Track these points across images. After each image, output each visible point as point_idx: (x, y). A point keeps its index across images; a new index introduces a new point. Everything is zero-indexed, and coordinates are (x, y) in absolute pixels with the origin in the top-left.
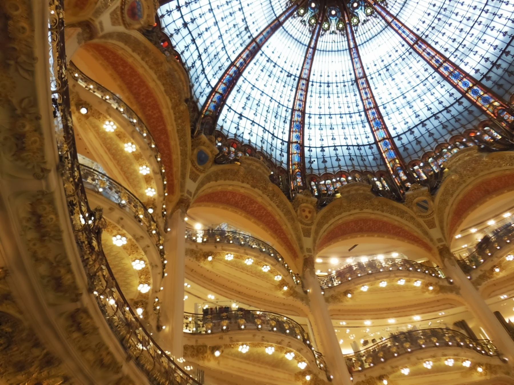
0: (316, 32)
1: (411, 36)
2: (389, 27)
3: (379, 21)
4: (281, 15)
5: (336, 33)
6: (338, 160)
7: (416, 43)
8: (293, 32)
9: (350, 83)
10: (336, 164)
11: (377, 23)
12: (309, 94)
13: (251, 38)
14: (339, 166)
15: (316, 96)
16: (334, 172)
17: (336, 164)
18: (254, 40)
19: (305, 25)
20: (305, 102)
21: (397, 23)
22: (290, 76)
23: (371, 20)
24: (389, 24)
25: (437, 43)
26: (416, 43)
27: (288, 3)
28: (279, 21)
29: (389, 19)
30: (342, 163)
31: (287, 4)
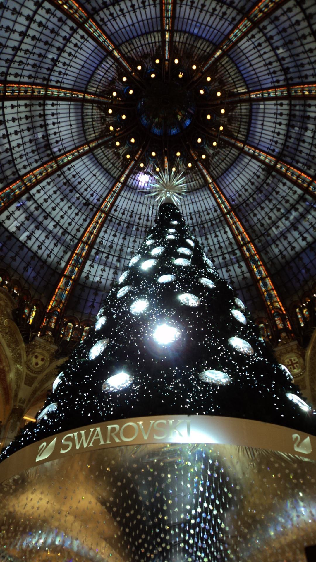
3: (198, 178)
8: (104, 161)
19: (119, 158)
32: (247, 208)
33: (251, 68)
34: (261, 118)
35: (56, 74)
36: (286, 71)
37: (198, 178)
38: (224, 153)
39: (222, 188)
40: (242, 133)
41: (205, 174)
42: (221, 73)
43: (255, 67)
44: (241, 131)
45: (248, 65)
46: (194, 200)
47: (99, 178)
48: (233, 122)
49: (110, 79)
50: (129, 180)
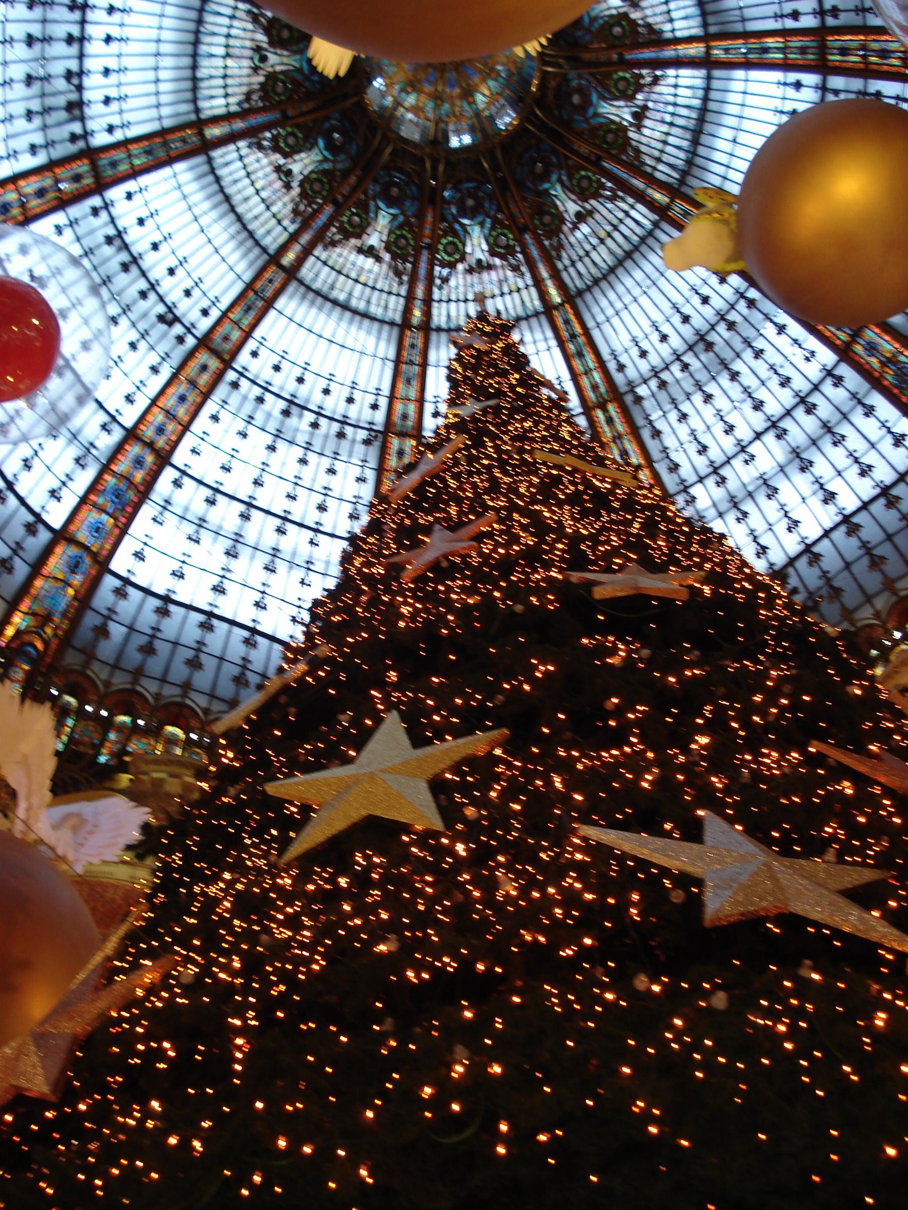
1: (597, 376)
5: (378, 259)
6: (195, 664)
7: (603, 407)
8: (240, 189)
9: (362, 434)
10: (179, 672)
11: (513, 288)
12: (210, 407)
13: (81, 144)
14: (187, 686)
15: (231, 423)
16: (157, 697)
17: (179, 672)
18: (91, 154)
20: (186, 428)
21: (572, 317)
22: (170, 324)
25: (657, 434)
27: (255, 97)
28: (201, 134)
29: (555, 296)
30: (202, 680)
31: (248, 96)
32: (662, 396)
37: (521, 284)
38: (610, 217)
39: (591, 324)
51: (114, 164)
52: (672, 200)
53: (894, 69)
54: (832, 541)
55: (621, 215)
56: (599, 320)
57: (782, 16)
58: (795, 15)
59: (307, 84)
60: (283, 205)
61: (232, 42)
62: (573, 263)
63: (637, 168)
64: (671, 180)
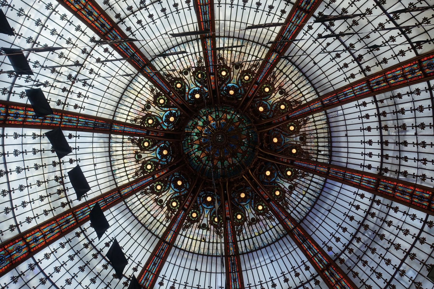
0: (179, 221)
2: (288, 236)
3: (274, 224)
4: (125, 186)
5: (208, 229)
11: (271, 227)
19: (162, 207)
22: (120, 279)
23: (264, 221)
24: (289, 232)
26: (327, 267)
33: (316, 67)
34: (343, 128)
35: (75, 96)
36: (358, 60)
38: (304, 184)
40: (322, 153)
41: (284, 217)
42: (280, 81)
43: (320, 64)
44: (320, 151)
45: (312, 64)
46: (273, 259)
47: (135, 238)
48: (307, 140)
49: (144, 103)
50: (178, 239)
51: (83, 213)
52: (329, 169)
53: (402, 82)
54: (425, 232)
55: (309, 182)
56: (314, 231)
57: (347, 78)
58: (353, 76)
59: (161, 162)
60: (162, 216)
61: (125, 152)
62: (294, 209)
63: (308, 160)
64: (325, 161)
